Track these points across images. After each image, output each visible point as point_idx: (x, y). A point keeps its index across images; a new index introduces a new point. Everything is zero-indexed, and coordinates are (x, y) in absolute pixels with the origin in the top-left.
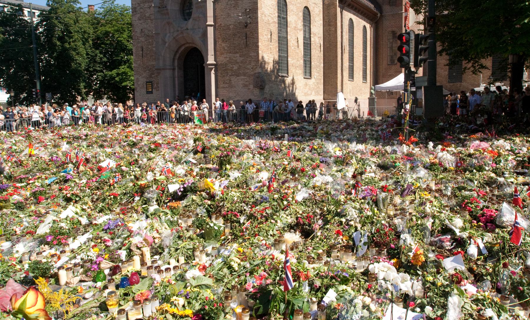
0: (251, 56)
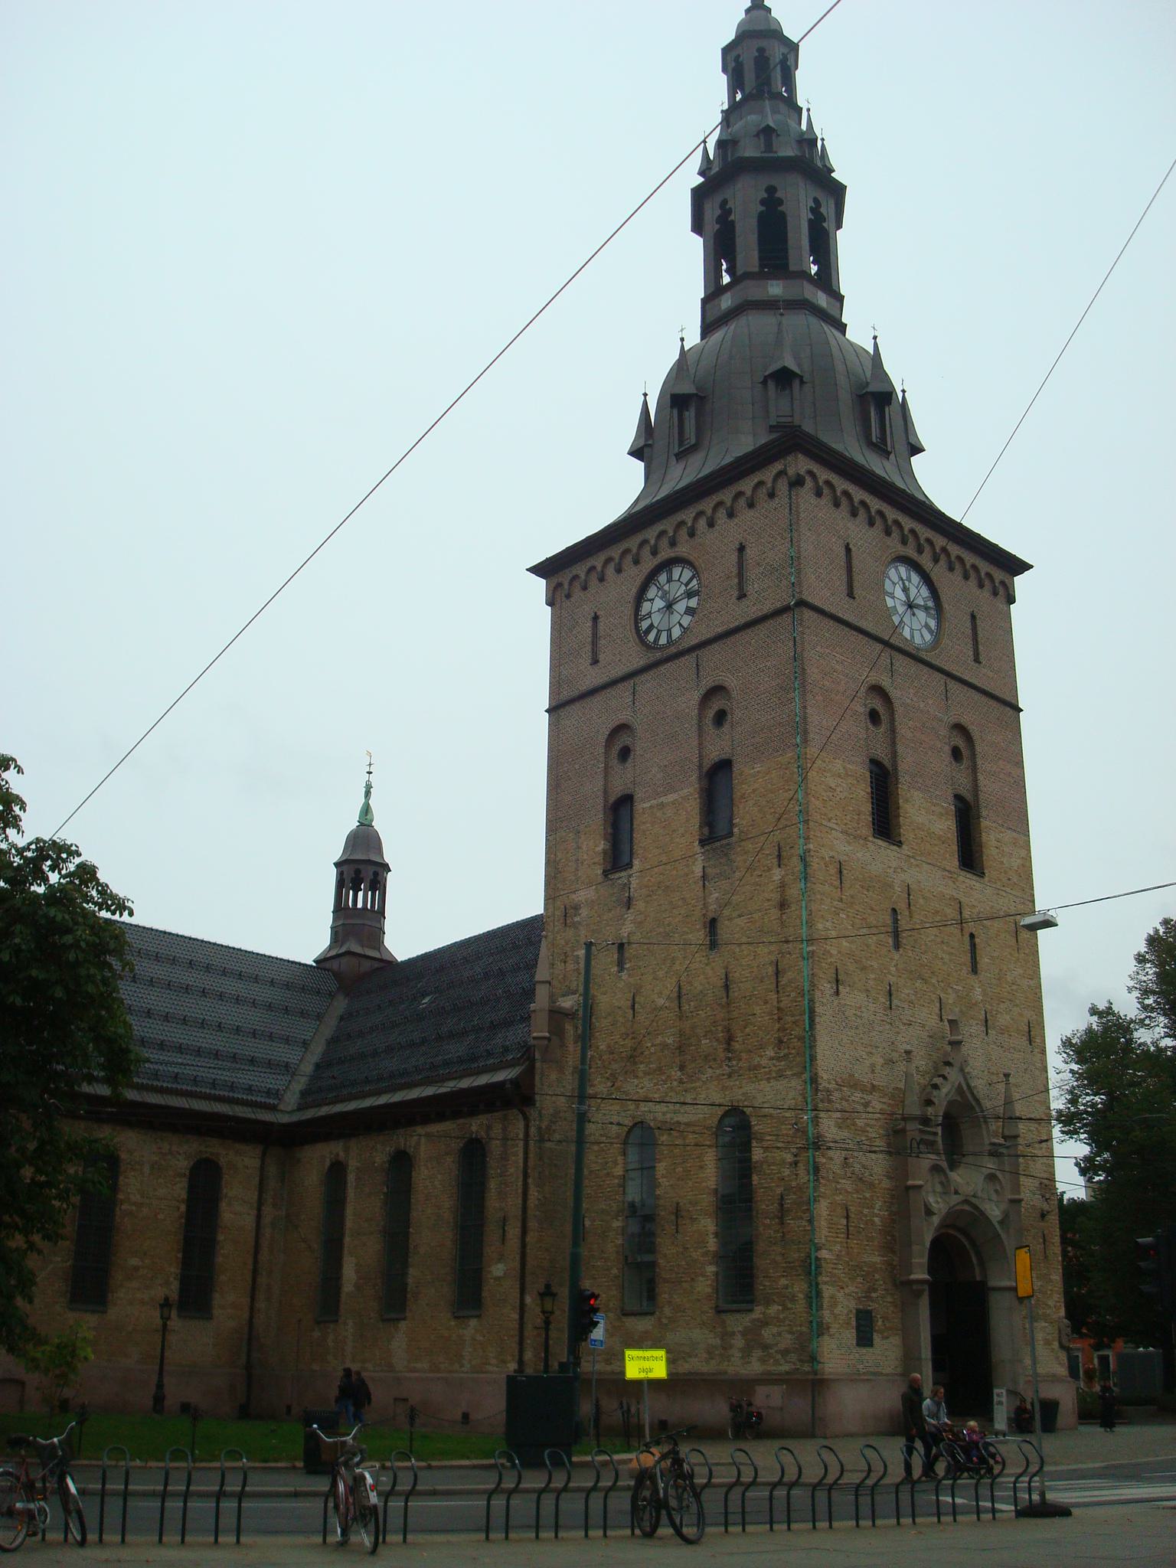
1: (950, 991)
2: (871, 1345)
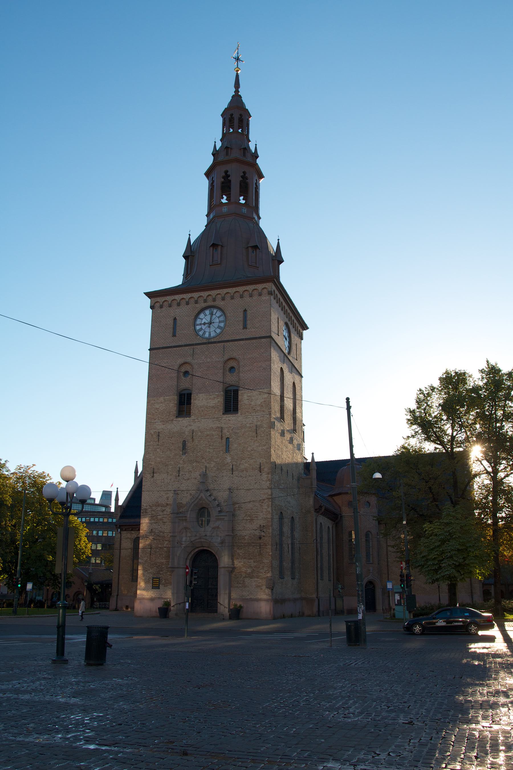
1: (213, 462)
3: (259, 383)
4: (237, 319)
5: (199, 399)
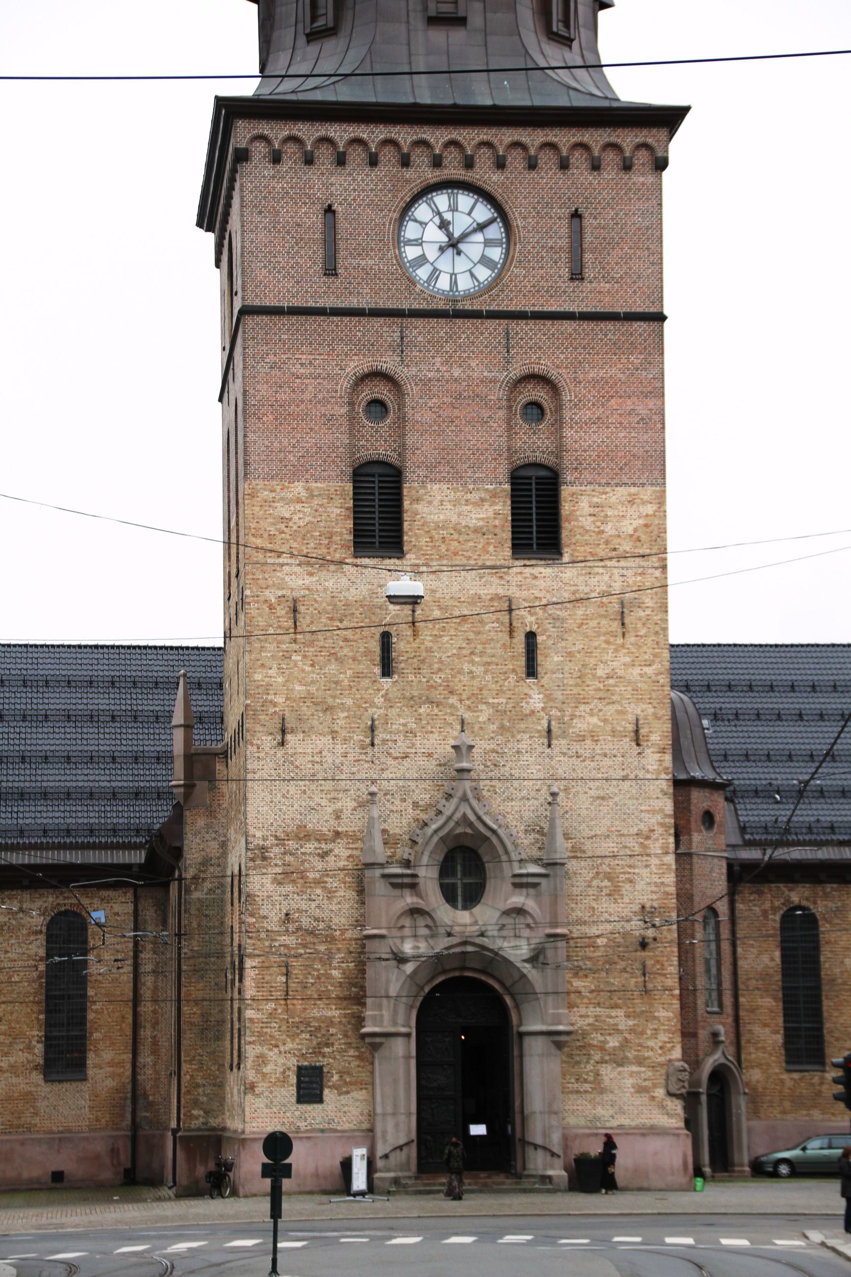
0: (655, 1018)
1: (484, 707)
2: (320, 1100)
3: (626, 464)
4: (550, 243)
5: (430, 499)
